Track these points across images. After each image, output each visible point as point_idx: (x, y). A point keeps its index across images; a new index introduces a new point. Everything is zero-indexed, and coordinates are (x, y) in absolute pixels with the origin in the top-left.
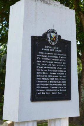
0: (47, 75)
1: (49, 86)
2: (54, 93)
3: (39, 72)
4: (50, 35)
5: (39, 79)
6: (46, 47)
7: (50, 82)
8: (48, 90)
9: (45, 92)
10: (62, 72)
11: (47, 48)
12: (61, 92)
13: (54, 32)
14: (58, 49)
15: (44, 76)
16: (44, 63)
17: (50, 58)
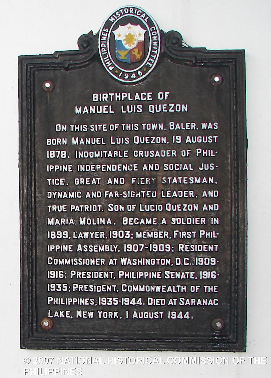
0: (106, 228)
1: (116, 280)
2: (146, 315)
3: (57, 215)
4: (113, 35)
5: (58, 247)
6: (96, 97)
7: (124, 261)
8: (113, 301)
9: (96, 308)
10: (194, 214)
11: (100, 103)
12: (184, 309)
13: (135, 22)
14: (168, 101)
15: (86, 235)
16: (84, 175)
17: (121, 148)
